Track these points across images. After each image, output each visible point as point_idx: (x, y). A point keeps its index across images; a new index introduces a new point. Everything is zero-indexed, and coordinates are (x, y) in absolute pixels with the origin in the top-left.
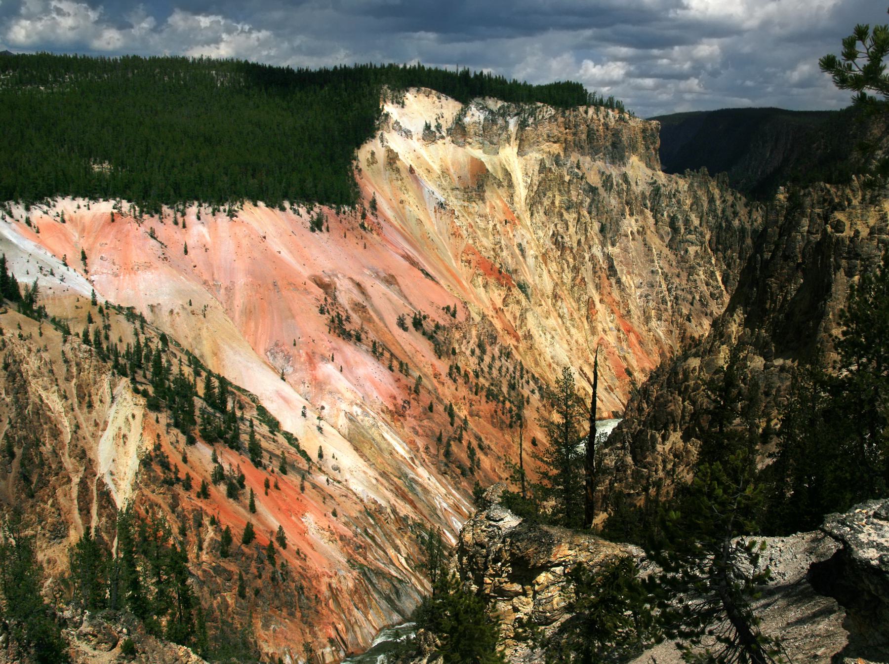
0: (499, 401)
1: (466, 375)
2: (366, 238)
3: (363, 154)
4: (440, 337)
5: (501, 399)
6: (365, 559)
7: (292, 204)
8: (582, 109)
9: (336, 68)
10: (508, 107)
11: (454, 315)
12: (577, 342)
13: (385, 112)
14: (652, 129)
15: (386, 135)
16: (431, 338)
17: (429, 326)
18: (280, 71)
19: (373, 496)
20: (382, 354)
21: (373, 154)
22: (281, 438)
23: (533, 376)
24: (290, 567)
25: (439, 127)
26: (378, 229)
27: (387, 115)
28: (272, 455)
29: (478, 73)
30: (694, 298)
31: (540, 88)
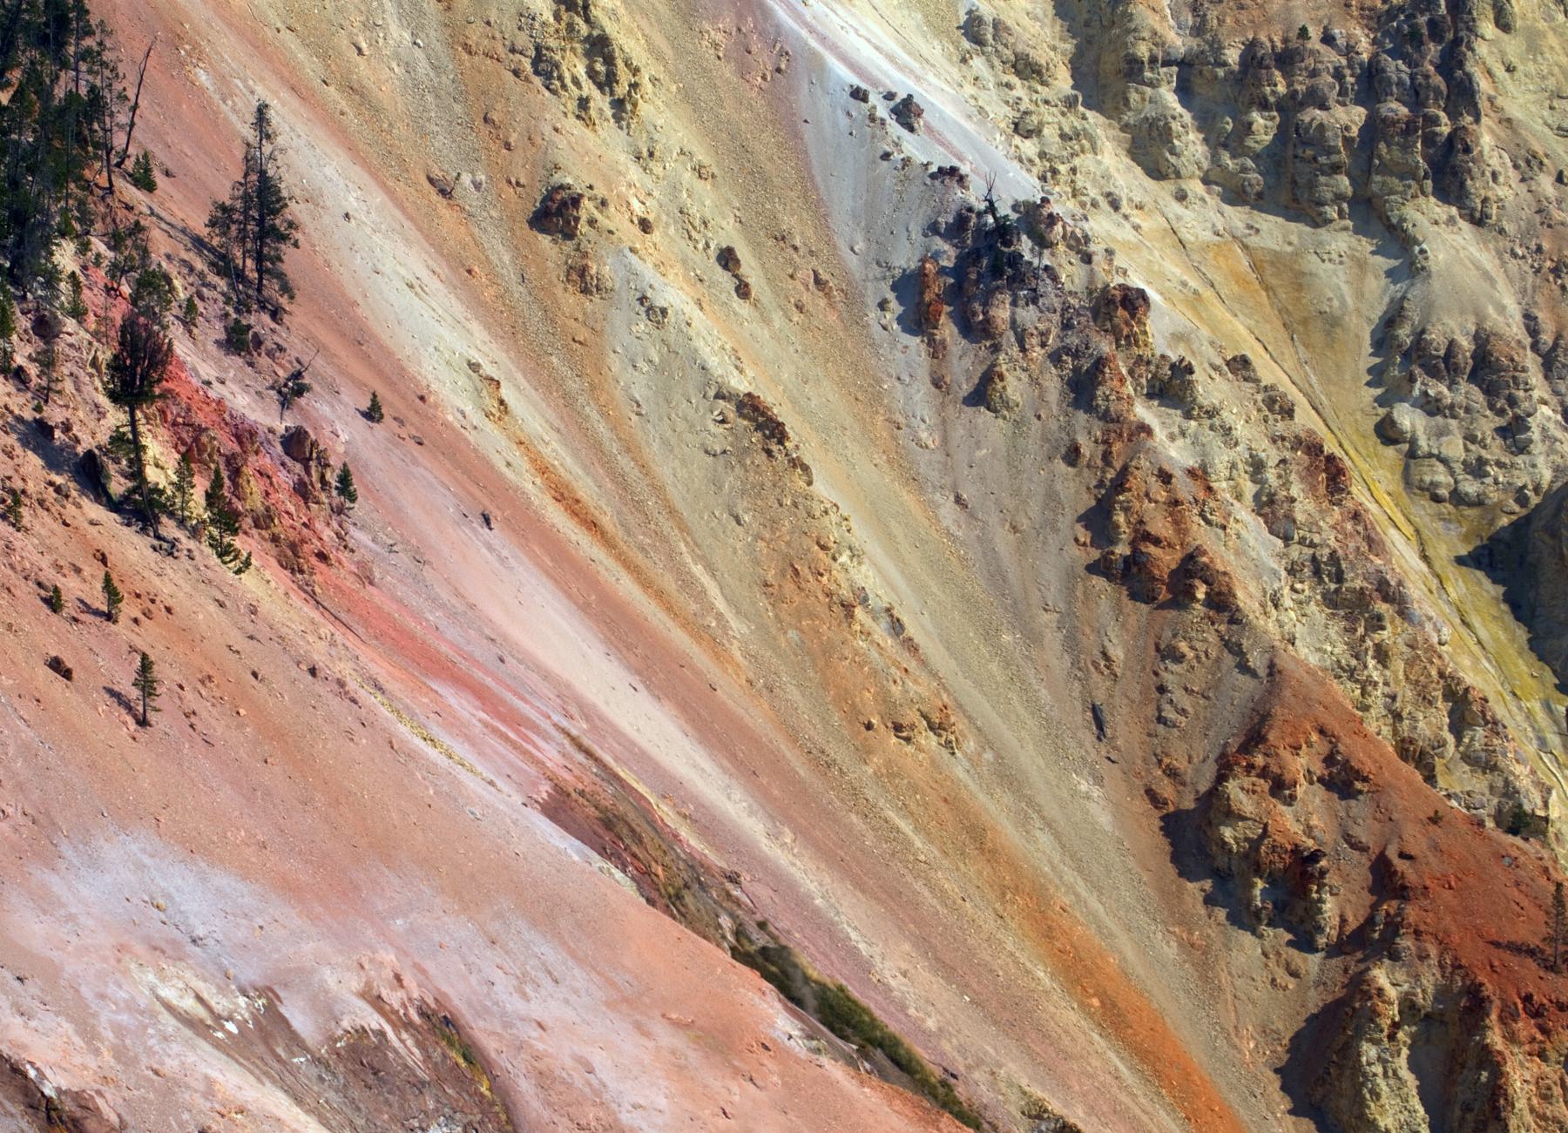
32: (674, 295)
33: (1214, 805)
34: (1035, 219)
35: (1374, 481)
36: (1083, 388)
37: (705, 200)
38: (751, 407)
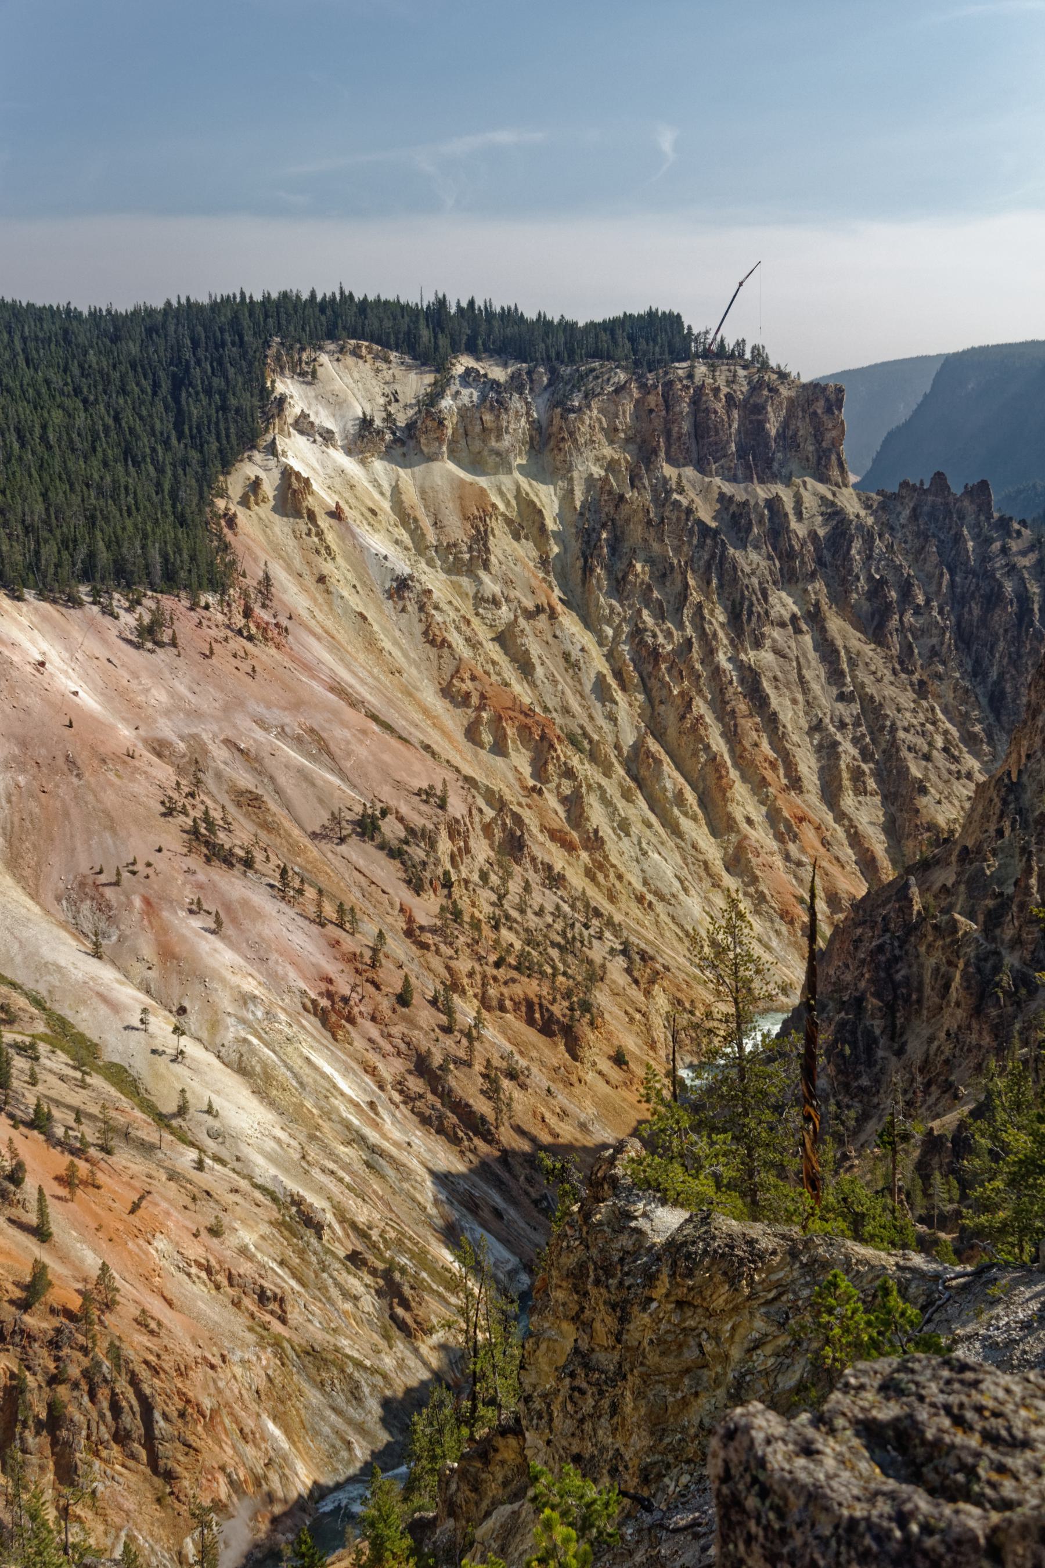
0: (543, 973)
1: (476, 925)
2: (254, 657)
3: (235, 484)
4: (417, 852)
5: (549, 971)
6: (283, 1321)
7: (95, 594)
8: (681, 368)
9: (168, 303)
10: (529, 373)
11: (442, 806)
12: (694, 847)
13: (276, 394)
14: (827, 400)
15: (281, 444)
16: (395, 854)
17: (391, 829)
18: (52, 312)
19: (295, 1187)
20: (300, 892)
21: (256, 485)
22: (96, 1080)
23: (610, 923)
24: (128, 1352)
25: (389, 418)
26: (274, 634)
27: (282, 400)
28: (79, 1115)
29: (464, 304)
30: (930, 744)
31: (592, 326)
32: (345, 594)
33: (450, 683)
34: (411, 577)
35: (475, 621)
36: (422, 608)
37: (349, 576)
38: (361, 614)
